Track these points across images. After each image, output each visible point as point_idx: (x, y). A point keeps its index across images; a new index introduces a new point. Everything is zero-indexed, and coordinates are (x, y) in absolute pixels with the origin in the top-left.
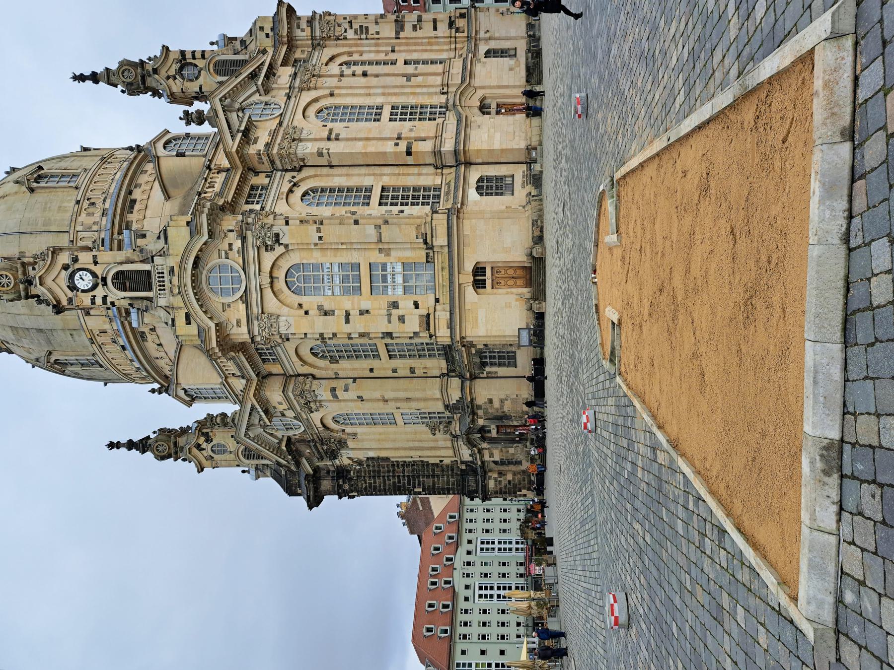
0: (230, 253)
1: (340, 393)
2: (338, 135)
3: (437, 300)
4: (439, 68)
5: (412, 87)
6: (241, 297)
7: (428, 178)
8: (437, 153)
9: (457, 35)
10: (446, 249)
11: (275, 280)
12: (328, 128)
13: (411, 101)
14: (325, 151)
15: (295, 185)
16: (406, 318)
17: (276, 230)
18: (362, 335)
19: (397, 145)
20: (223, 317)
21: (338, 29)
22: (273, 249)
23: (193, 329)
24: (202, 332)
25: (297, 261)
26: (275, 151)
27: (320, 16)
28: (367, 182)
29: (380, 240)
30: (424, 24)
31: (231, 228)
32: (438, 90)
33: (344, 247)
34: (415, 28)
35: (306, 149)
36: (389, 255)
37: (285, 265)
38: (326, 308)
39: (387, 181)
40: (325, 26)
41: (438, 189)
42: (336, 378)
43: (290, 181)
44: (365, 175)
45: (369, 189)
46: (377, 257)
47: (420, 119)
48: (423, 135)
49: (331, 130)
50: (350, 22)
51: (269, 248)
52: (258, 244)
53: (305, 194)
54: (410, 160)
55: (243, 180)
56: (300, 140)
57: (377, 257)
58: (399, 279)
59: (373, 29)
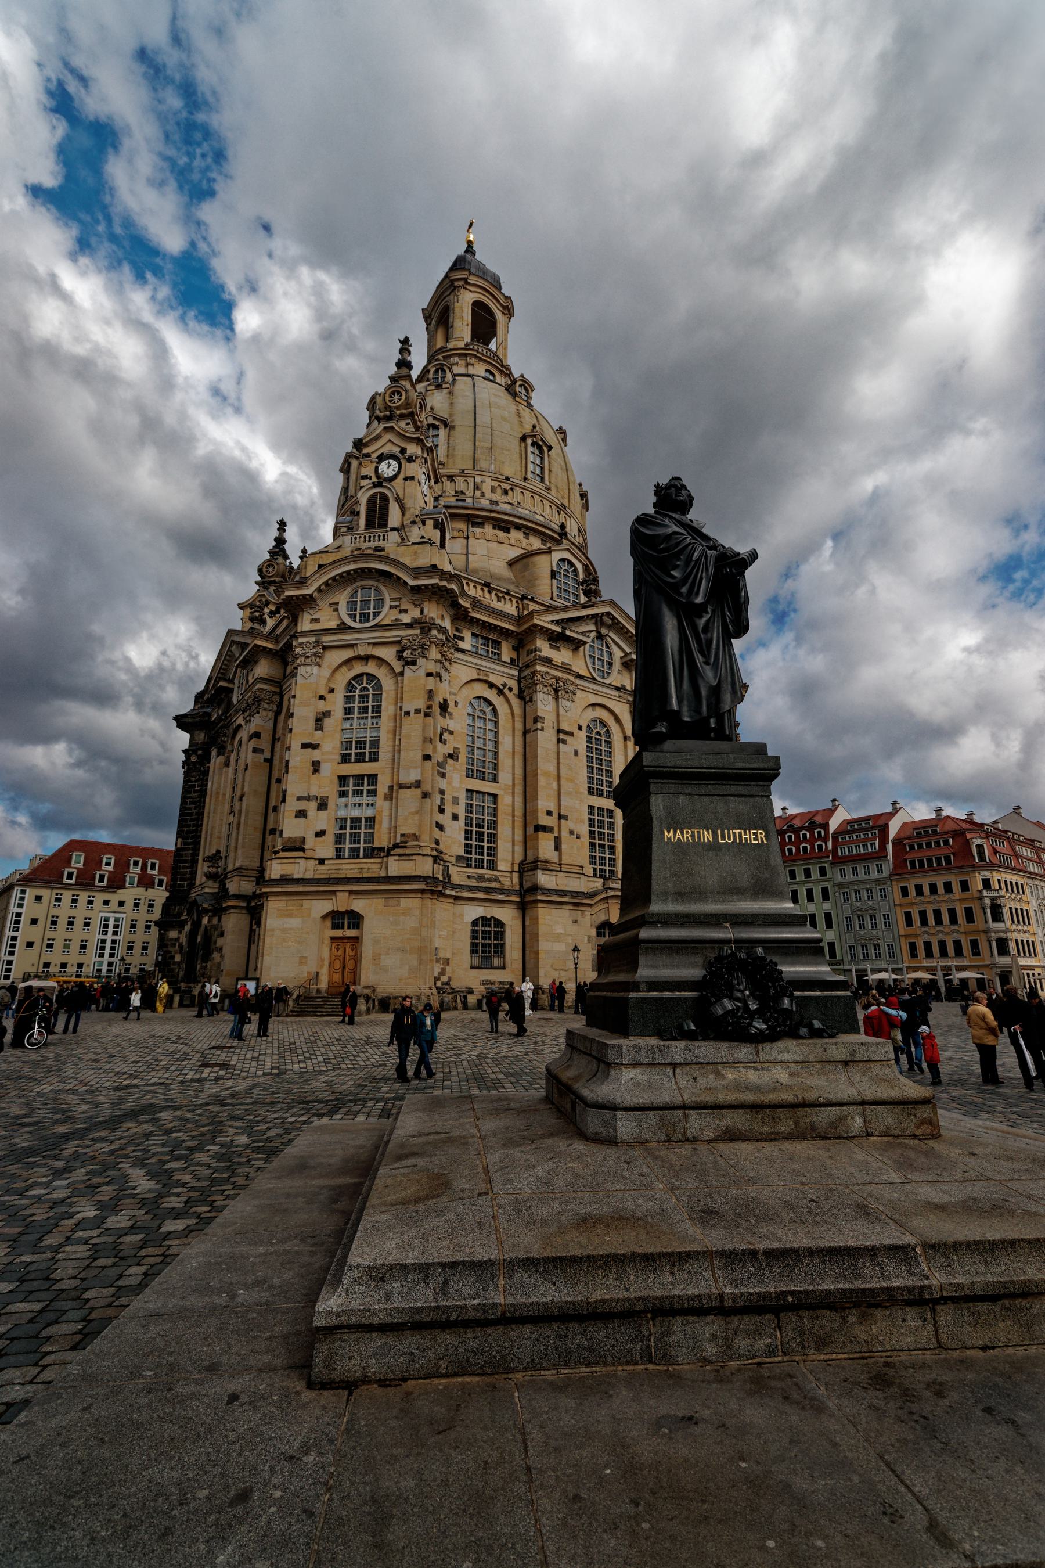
0: (396, 611)
2: (564, 742)
3: (322, 862)
6: (344, 623)
7: (508, 853)
10: (383, 874)
11: (364, 663)
12: (576, 731)
14: (539, 725)
15: (500, 692)
16: (303, 820)
17: (421, 661)
19: (549, 813)
20: (323, 604)
22: (400, 657)
25: (385, 687)
26: (539, 668)
29: (401, 786)
31: (425, 612)
33: (397, 743)
36: (389, 797)
37: (381, 673)
38: (327, 722)
39: (505, 801)
41: (492, 865)
42: (274, 740)
43: (504, 685)
44: (514, 774)
45: (495, 780)
47: (592, 845)
48: (564, 847)
49: (571, 734)
52: (404, 642)
53: (489, 703)
54: (530, 830)
55: (505, 633)
56: (557, 698)
58: (356, 813)
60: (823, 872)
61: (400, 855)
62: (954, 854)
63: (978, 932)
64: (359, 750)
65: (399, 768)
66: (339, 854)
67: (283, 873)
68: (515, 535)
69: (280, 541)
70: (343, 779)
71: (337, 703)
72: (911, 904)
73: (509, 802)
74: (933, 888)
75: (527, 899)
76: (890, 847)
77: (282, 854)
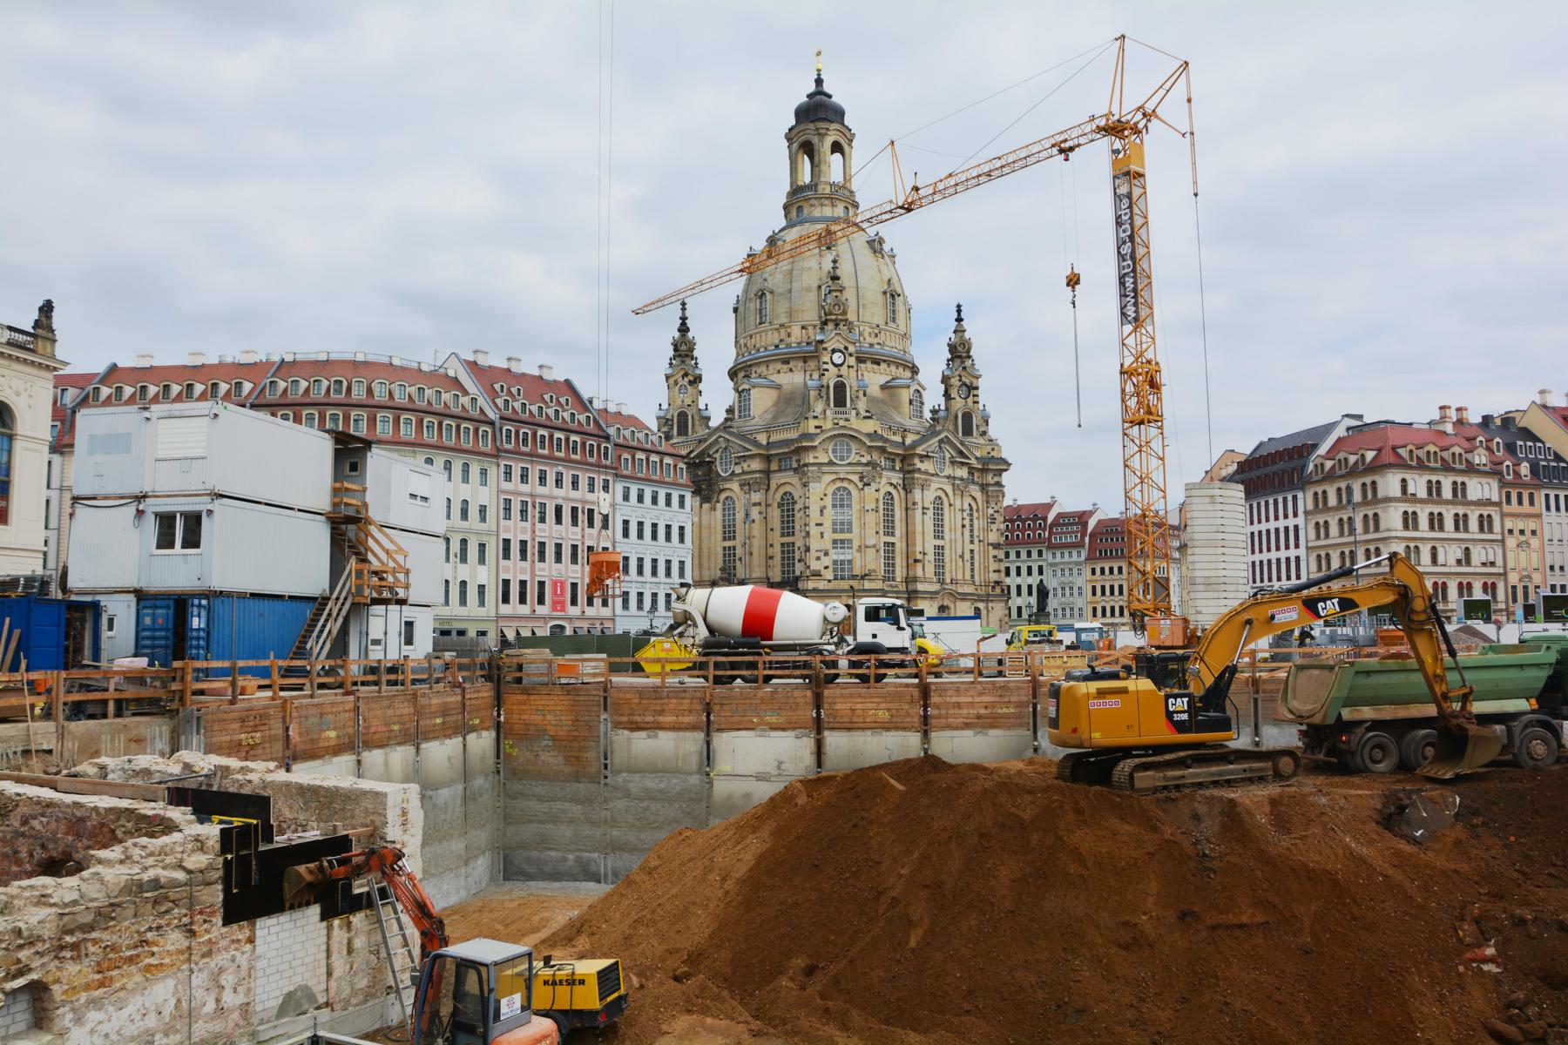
1: (757, 508)
4: (968, 577)
7: (900, 573)
8: (915, 580)
13: (947, 559)
18: (808, 533)
23: (812, 430)
24: (811, 437)
28: (898, 533)
35: (917, 493)
37: (851, 487)
39: (898, 546)
42: (767, 505)
45: (893, 534)
46: (855, 545)
51: (861, 479)
57: (855, 545)
58: (842, 557)
59: (994, 527)
60: (1040, 553)
64: (842, 527)
68: (883, 366)
69: (684, 319)
70: (835, 542)
71: (828, 501)
73: (900, 546)
74: (1111, 570)
76: (1087, 539)
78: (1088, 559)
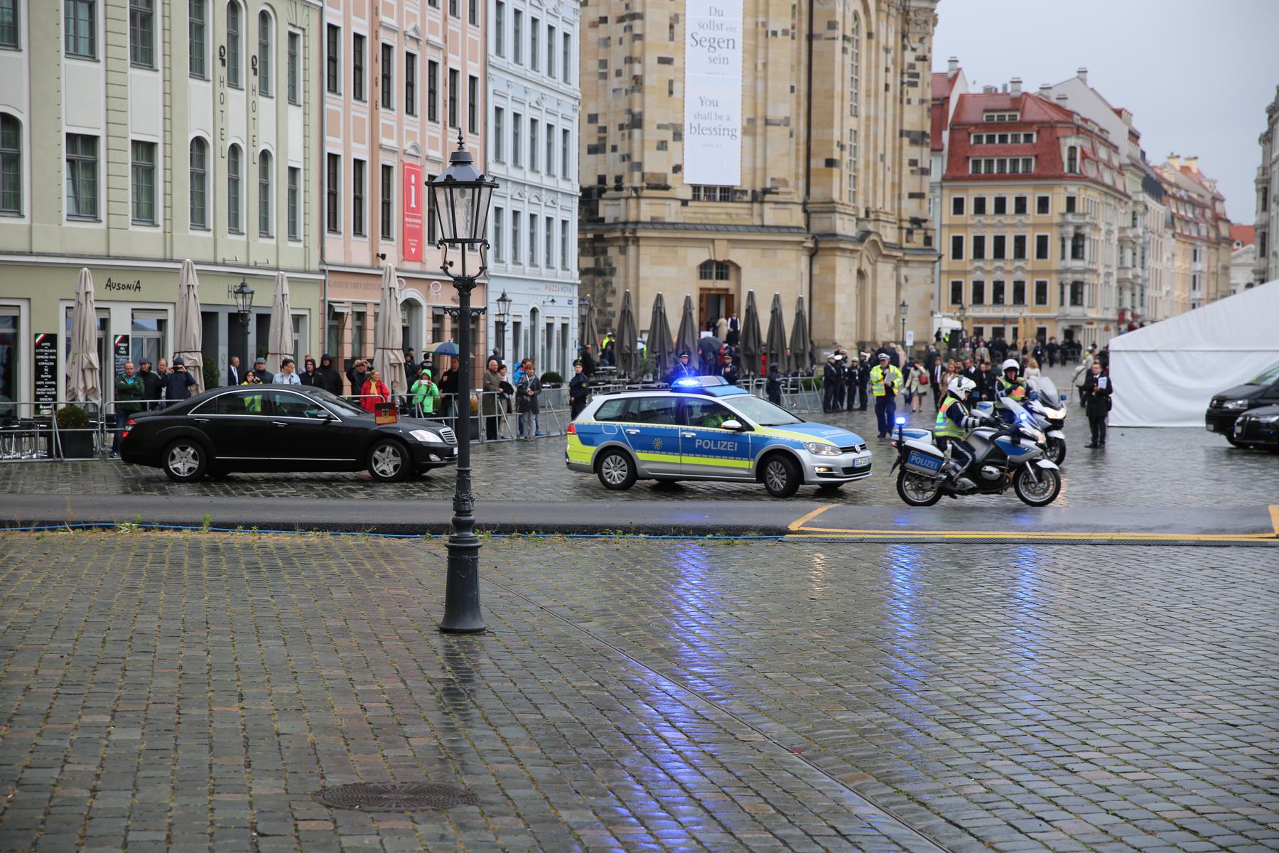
3: (685, 203)
5: (875, 164)
9: (904, 232)
10: (757, 222)
18: (638, 81)
21: (917, 38)
27: (933, 10)
29: (767, 122)
30: (917, 177)
32: (870, 205)
33: (760, 67)
34: (913, 163)
40: (922, 17)
50: (924, 59)
59: (914, 94)
61: (776, 203)
62: (1036, 156)
63: (1049, 272)
65: (766, 99)
66: (696, 197)
67: (654, 214)
72: (966, 226)
74: (1000, 205)
75: (821, 245)
76: (946, 135)
77: (646, 193)
78: (953, 176)
